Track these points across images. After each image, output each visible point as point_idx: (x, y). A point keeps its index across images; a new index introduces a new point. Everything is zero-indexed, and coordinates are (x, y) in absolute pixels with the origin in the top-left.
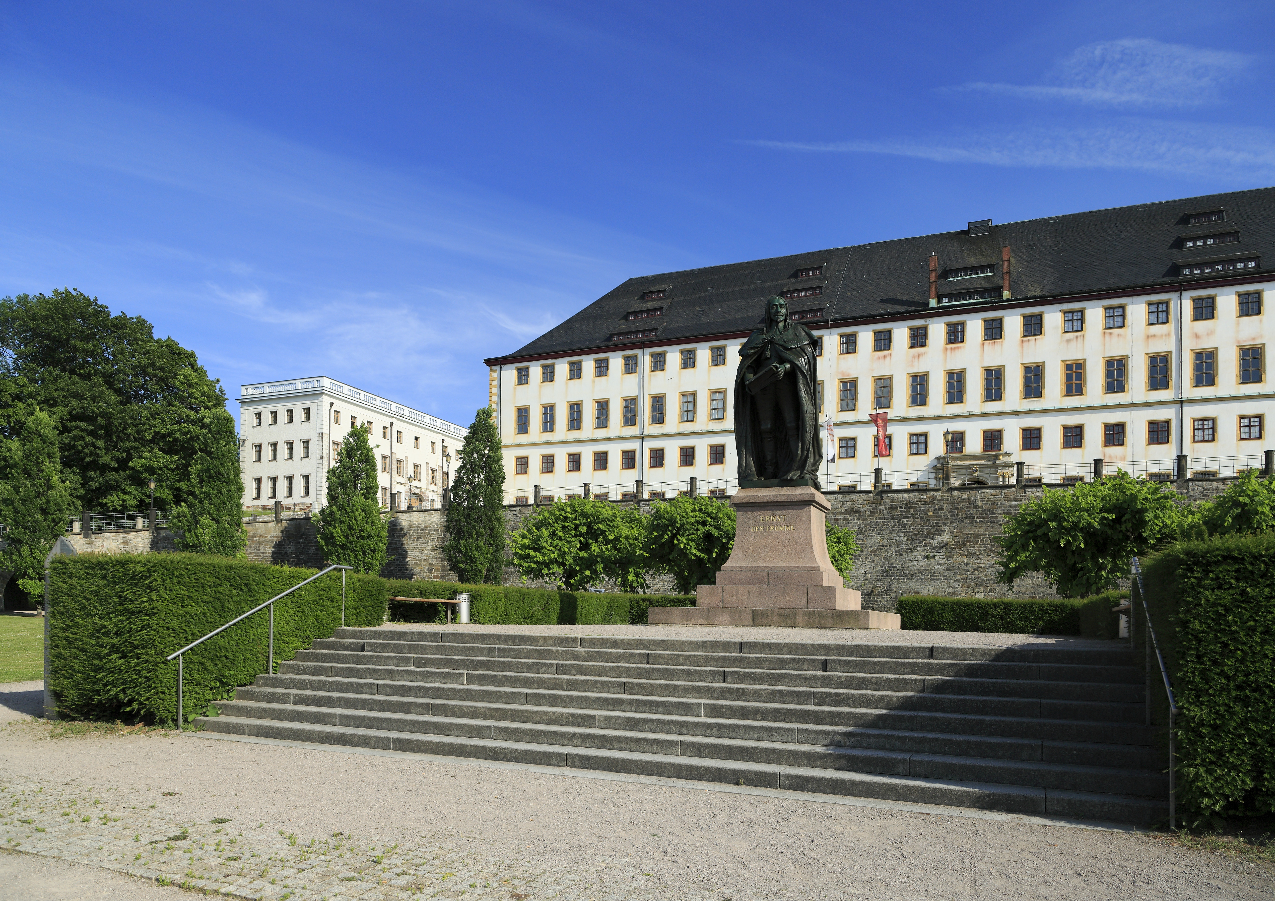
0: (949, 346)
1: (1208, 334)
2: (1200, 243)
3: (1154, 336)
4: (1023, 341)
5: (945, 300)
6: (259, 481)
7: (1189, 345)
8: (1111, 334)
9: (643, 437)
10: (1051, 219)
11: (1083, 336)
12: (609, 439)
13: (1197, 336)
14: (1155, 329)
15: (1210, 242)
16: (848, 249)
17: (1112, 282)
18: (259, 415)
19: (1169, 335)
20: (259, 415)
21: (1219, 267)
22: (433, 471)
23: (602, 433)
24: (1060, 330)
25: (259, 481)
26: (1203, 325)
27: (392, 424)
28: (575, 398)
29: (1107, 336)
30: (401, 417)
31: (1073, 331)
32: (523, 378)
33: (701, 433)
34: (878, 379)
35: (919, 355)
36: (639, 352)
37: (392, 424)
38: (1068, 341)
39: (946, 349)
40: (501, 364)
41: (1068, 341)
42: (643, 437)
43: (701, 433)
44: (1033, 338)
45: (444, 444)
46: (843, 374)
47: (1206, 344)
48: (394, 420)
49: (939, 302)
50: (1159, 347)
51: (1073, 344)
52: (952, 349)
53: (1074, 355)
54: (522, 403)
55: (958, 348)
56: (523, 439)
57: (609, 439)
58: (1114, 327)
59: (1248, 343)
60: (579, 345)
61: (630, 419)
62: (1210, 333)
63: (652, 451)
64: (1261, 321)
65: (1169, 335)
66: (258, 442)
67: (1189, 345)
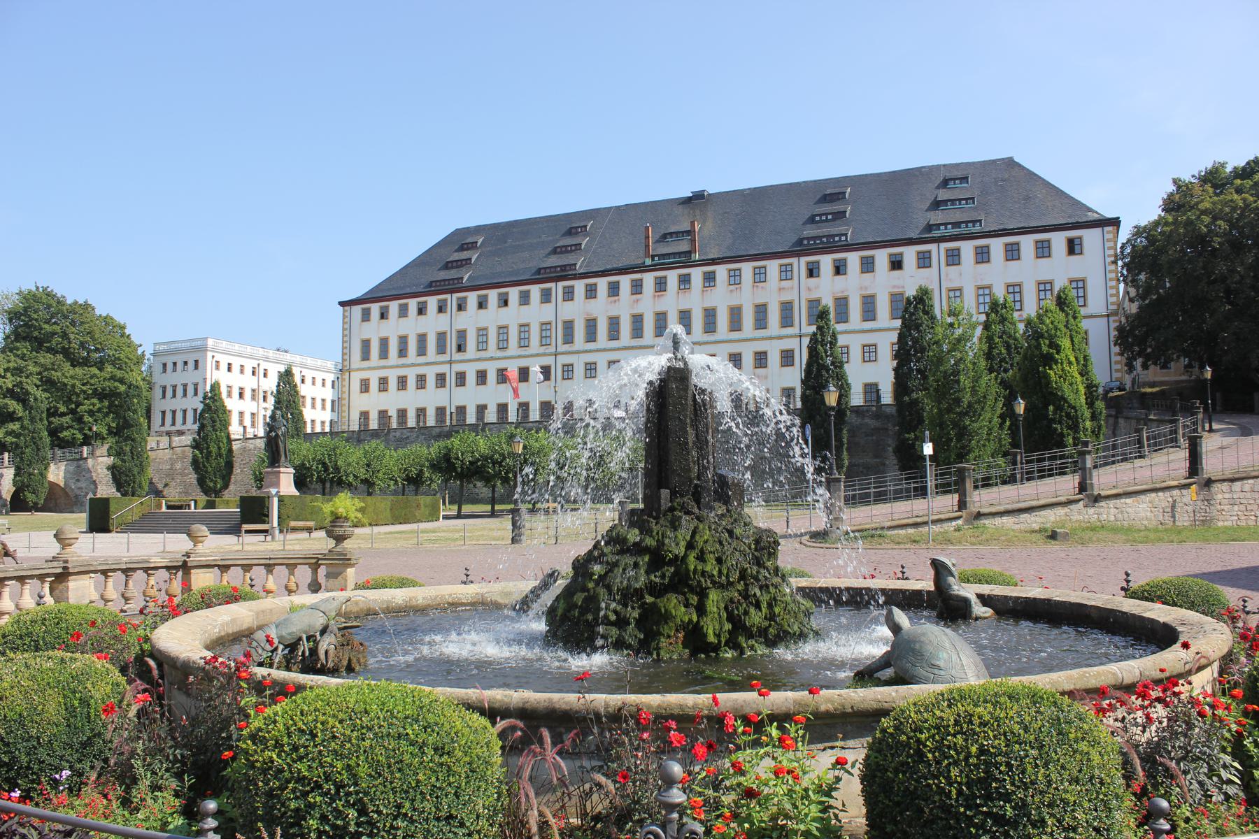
2: (824, 218)
5: (656, 258)
6: (164, 413)
7: (805, 295)
9: (451, 362)
10: (745, 190)
12: (427, 364)
13: (809, 289)
14: (784, 284)
15: (830, 217)
16: (611, 208)
17: (762, 249)
18: (165, 365)
19: (792, 288)
20: (165, 365)
21: (824, 240)
23: (422, 359)
24: (727, 283)
25: (164, 413)
28: (402, 333)
30: (267, 359)
32: (366, 316)
33: (492, 358)
34: (611, 318)
38: (731, 291)
41: (731, 291)
42: (451, 362)
43: (492, 358)
47: (814, 296)
48: (261, 362)
49: (653, 260)
50: (786, 297)
51: (734, 293)
53: (735, 302)
54: (365, 337)
56: (366, 364)
57: (427, 364)
59: (840, 295)
60: (408, 290)
61: (441, 349)
62: (817, 287)
65: (792, 288)
66: (163, 384)
67: (805, 295)
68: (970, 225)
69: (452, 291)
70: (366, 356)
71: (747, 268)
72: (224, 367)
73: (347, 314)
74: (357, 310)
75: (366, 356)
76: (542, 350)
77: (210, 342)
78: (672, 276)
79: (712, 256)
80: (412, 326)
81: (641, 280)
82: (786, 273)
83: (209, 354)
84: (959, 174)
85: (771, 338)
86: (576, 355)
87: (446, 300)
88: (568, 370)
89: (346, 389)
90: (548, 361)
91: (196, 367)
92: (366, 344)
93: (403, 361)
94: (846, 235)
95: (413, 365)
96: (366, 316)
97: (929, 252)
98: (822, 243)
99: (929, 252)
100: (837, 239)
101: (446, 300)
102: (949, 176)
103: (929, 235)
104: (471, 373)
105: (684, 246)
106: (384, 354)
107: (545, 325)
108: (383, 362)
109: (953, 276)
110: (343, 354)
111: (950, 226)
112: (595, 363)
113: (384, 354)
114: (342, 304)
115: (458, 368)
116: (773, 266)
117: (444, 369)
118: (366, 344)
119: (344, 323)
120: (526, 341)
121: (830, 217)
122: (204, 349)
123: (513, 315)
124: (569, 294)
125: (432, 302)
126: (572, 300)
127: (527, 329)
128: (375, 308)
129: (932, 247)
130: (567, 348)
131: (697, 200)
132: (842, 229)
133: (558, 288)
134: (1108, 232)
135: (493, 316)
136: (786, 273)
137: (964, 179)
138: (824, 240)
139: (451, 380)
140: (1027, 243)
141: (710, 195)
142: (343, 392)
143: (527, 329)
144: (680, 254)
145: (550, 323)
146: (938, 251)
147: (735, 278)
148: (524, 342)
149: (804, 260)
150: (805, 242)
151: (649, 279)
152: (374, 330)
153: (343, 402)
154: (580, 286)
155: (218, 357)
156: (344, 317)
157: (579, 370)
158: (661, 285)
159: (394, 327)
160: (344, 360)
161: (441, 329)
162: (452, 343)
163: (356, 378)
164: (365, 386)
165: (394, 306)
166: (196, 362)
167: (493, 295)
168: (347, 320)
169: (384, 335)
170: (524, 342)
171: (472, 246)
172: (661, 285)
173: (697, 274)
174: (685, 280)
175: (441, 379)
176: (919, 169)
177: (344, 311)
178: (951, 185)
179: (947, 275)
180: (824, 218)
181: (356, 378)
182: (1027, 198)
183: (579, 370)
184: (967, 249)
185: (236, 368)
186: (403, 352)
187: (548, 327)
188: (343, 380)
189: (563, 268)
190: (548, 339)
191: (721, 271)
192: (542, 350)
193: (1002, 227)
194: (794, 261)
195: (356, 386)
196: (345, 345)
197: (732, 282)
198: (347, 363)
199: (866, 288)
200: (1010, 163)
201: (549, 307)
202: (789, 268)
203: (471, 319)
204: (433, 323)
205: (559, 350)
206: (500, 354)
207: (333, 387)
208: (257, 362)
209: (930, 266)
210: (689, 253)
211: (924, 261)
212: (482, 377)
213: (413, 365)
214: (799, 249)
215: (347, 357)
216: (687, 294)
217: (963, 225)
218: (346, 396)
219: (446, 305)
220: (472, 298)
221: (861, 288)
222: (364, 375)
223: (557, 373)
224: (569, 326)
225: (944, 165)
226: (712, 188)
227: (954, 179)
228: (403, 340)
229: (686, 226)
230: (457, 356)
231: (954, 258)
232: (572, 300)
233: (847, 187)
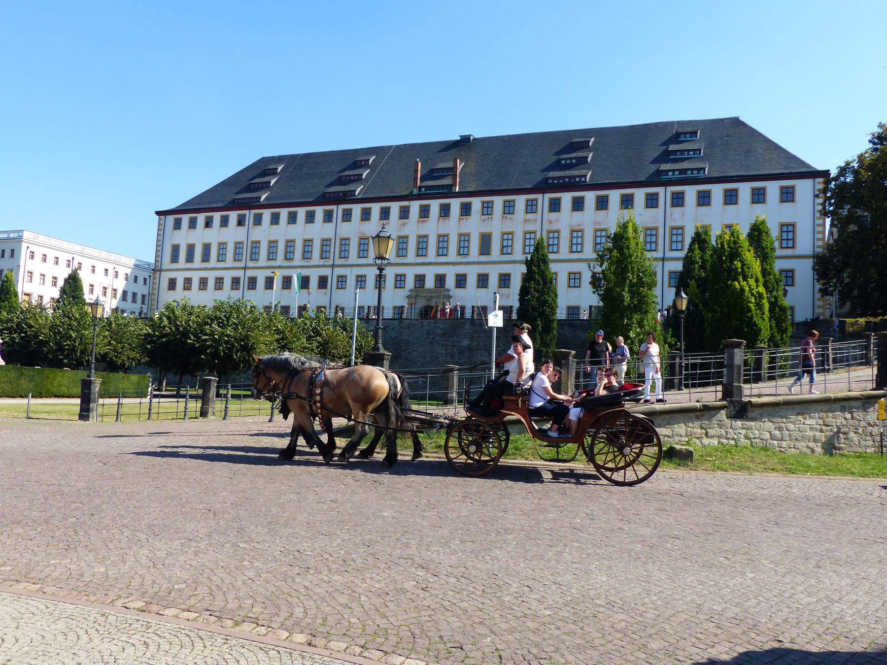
0: (421, 220)
1: (556, 221)
3: (528, 220)
4: (460, 219)
5: (423, 189)
8: (506, 217)
11: (492, 218)
13: (550, 222)
14: (530, 216)
16: (391, 147)
19: (536, 220)
22: (105, 288)
24: (480, 213)
26: (554, 215)
27: (73, 258)
28: (207, 241)
29: (504, 218)
30: (82, 255)
31: (487, 214)
32: (177, 225)
35: (404, 224)
36: (246, 212)
37: (73, 258)
38: (484, 220)
39: (419, 221)
40: (165, 215)
41: (484, 220)
42: (245, 268)
44: (465, 217)
45: (115, 270)
46: (362, 233)
51: (486, 222)
52: (422, 221)
53: (486, 230)
54: (176, 242)
55: (426, 221)
58: (509, 213)
60: (215, 205)
61: (237, 257)
62: (557, 221)
63: (250, 278)
64: (583, 215)
65: (536, 220)
67: (546, 227)
68: (695, 172)
69: (250, 208)
70: (175, 258)
71: (498, 201)
72: (38, 256)
73: (162, 222)
74: (170, 219)
75: (175, 258)
76: (322, 262)
77: (26, 235)
78: (435, 205)
79: (469, 189)
80: (214, 236)
81: (409, 207)
82: (531, 207)
83: (24, 245)
84: (690, 129)
85: (514, 262)
86: (349, 269)
87: (244, 215)
88: (342, 281)
89: (157, 286)
90: (326, 272)
91: (12, 255)
92: (176, 249)
93: (206, 265)
94: (585, 176)
95: (214, 269)
96: (177, 225)
97: (657, 194)
98: (565, 181)
99: (657, 194)
100: (578, 179)
101: (244, 215)
102: (680, 130)
103: (657, 179)
104: (261, 277)
105: (447, 181)
106: (190, 258)
107: (325, 242)
108: (189, 265)
109: (677, 216)
110: (156, 256)
111: (677, 173)
112: (365, 276)
113: (190, 258)
114: (158, 213)
115: (250, 273)
116: (520, 201)
117: (239, 273)
118: (176, 249)
119: (159, 230)
120: (309, 254)
121: (574, 161)
122: (19, 239)
123: (300, 231)
124: (347, 216)
125: (233, 216)
126: (350, 221)
127: (310, 244)
128: (185, 218)
129: (660, 190)
130: (341, 262)
131: (465, 141)
132: (583, 172)
133: (338, 210)
134: (819, 183)
135: (283, 232)
136: (531, 207)
137: (694, 133)
138: (567, 180)
139: (244, 283)
140: (745, 190)
141: (475, 139)
142: (154, 289)
143: (310, 244)
144: (443, 187)
145: (330, 240)
146: (664, 193)
147: (487, 209)
148: (307, 254)
149: (548, 196)
150: (550, 181)
151: (415, 206)
152: (183, 237)
153: (154, 297)
154: (357, 209)
155: (32, 248)
156: (159, 224)
157: (351, 282)
158: (425, 212)
159: (199, 236)
160: (156, 261)
161: (239, 240)
162: (246, 251)
163: (165, 277)
164: (172, 284)
165: (201, 218)
166: (13, 251)
167: (284, 213)
168: (162, 227)
169: (191, 242)
170: (307, 254)
171: (273, 172)
172: (425, 212)
173: (455, 204)
174: (445, 211)
175: (236, 281)
176: (656, 124)
177: (160, 220)
178: (682, 138)
179: (671, 214)
180: (569, 162)
181: (165, 277)
182: (748, 151)
183: (351, 282)
184: (691, 192)
185: (50, 259)
186: (206, 257)
187: (328, 243)
188: (155, 278)
189: (345, 193)
190: (328, 253)
191: (476, 203)
192: (322, 262)
193: (722, 175)
194: (539, 196)
195: (165, 284)
196: (159, 248)
197: (485, 212)
198: (159, 264)
199: (599, 224)
200: (736, 123)
201: (330, 226)
202: (534, 203)
203: (264, 233)
204: (233, 234)
205: (335, 263)
206: (286, 264)
207: (145, 284)
208: (73, 256)
209: (657, 207)
210: (450, 187)
211: (652, 201)
212: (269, 283)
213: (214, 269)
214: (543, 187)
215: (159, 259)
216: (447, 221)
217: (689, 172)
218: (156, 292)
219: (245, 219)
220: (267, 214)
221: (595, 223)
222: (173, 275)
223: (332, 282)
224: (345, 242)
225: (677, 122)
226: (478, 132)
227: (685, 133)
228: (207, 248)
229: (451, 165)
230: (250, 264)
231: (678, 200)
232: (350, 221)
233: (591, 137)
